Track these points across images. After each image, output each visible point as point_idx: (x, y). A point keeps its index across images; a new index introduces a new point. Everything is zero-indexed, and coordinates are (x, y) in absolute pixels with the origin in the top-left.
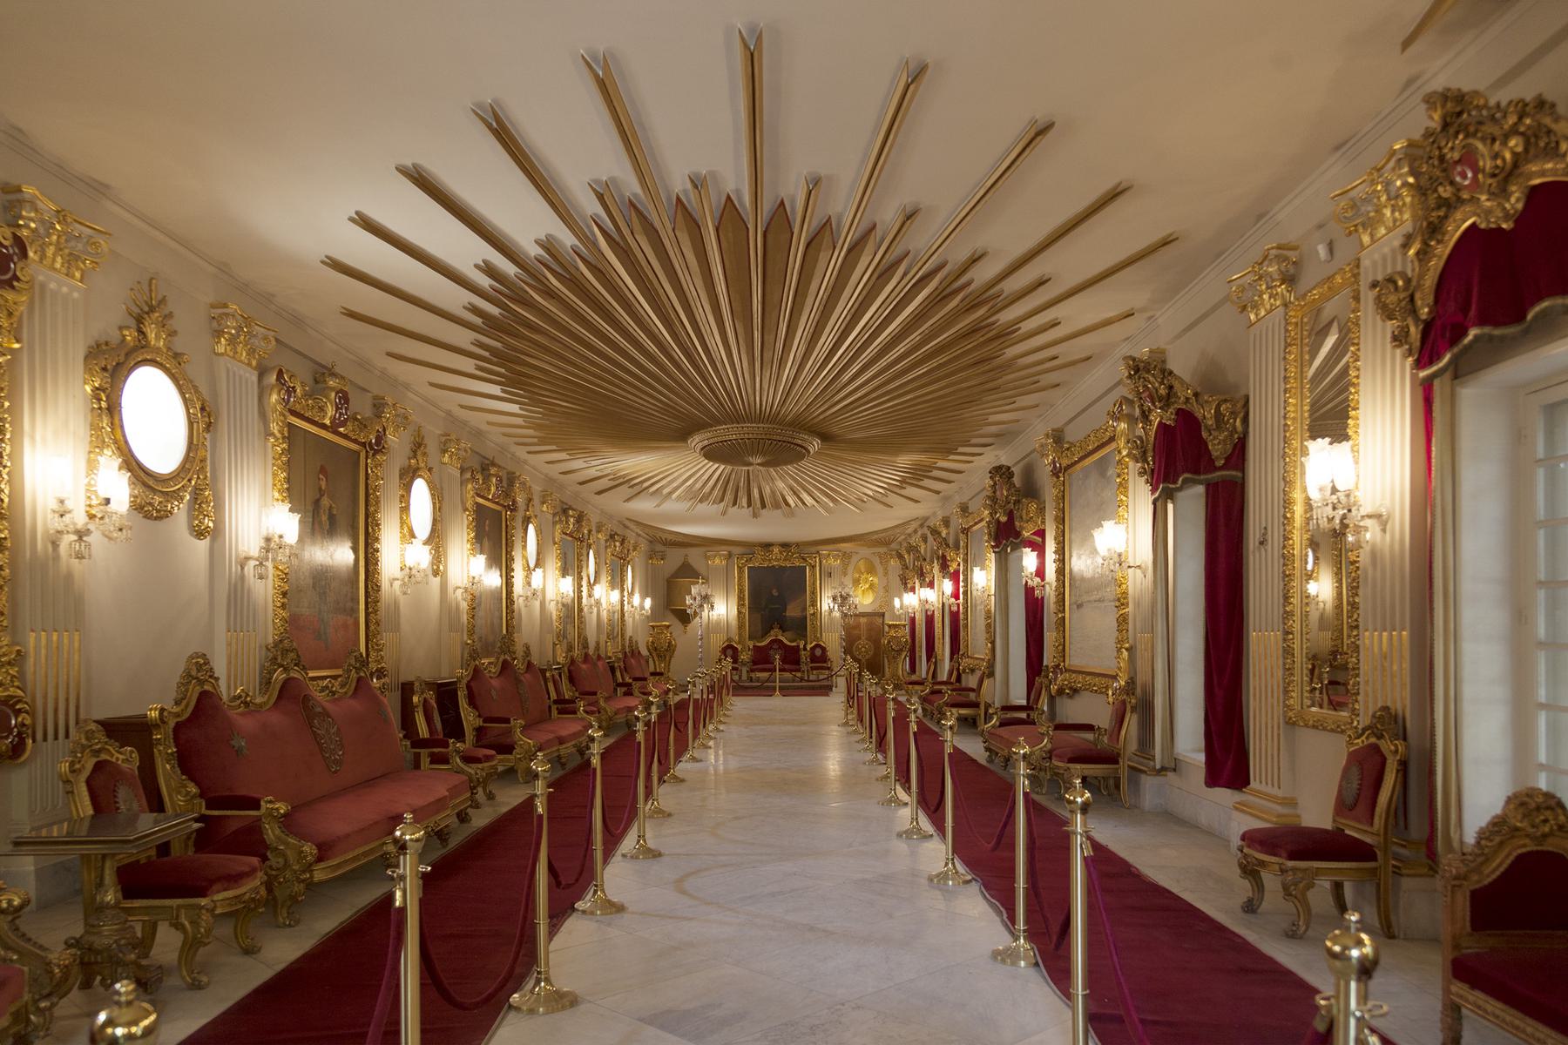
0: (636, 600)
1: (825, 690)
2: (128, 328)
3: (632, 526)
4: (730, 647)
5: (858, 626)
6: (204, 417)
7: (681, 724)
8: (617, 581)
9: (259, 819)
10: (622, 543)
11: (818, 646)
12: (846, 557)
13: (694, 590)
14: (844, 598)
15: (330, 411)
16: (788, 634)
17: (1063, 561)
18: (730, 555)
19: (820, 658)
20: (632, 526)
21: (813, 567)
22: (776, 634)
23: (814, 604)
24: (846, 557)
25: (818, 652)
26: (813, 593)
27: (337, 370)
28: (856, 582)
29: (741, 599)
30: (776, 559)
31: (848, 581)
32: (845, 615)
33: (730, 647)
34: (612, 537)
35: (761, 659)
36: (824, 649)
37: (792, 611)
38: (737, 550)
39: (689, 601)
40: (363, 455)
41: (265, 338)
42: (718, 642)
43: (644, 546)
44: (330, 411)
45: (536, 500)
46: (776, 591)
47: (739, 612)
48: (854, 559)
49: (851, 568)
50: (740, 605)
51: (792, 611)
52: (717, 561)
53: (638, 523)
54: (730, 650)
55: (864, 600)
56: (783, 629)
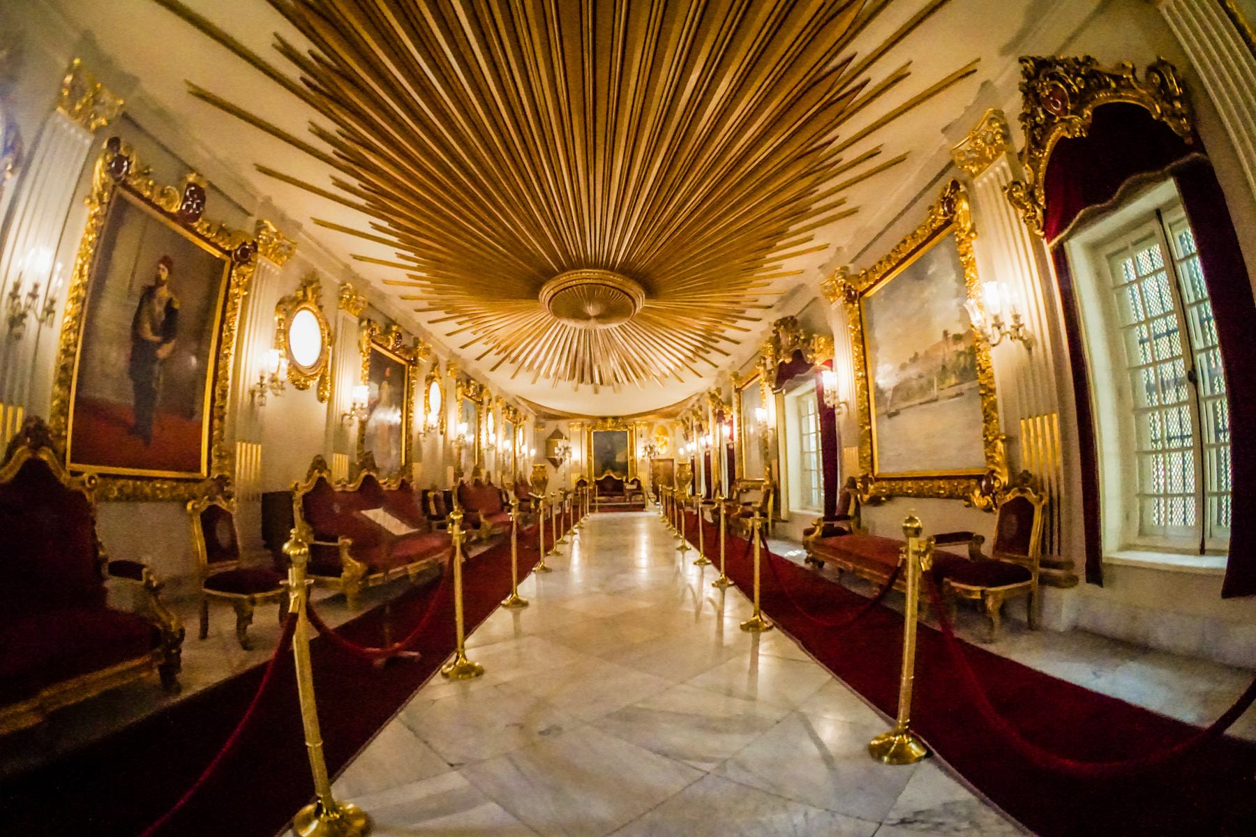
0: (525, 449)
10: (515, 412)
38: (587, 421)
39: (556, 451)
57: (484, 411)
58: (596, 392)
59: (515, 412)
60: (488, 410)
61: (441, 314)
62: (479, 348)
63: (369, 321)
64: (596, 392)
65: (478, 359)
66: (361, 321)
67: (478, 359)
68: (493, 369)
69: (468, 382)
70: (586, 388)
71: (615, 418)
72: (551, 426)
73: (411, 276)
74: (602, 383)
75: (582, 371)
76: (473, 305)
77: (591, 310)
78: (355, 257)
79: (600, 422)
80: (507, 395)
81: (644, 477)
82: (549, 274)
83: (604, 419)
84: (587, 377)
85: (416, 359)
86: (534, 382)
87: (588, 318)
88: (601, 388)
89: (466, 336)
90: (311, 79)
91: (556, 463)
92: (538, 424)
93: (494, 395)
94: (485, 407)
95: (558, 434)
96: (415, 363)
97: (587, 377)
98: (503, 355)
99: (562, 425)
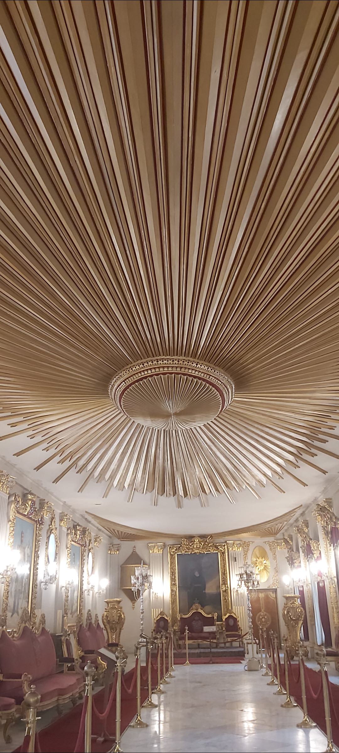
10: (84, 531)
38: (170, 542)
39: (133, 580)
57: (44, 533)
58: (179, 505)
59: (84, 531)
60: (50, 531)
62: (39, 455)
64: (179, 505)
65: (38, 468)
67: (38, 468)
68: (56, 481)
69: (25, 496)
70: (168, 501)
71: (203, 537)
72: (127, 547)
75: (163, 481)
76: (29, 403)
77: (169, 407)
79: (185, 542)
80: (74, 511)
81: (242, 613)
82: (120, 364)
83: (190, 538)
84: (168, 488)
86: (105, 495)
88: (185, 501)
89: (23, 441)
91: (133, 596)
92: (111, 547)
93: (58, 512)
94: (45, 527)
95: (135, 559)
97: (168, 488)
98: (67, 463)
99: (140, 546)
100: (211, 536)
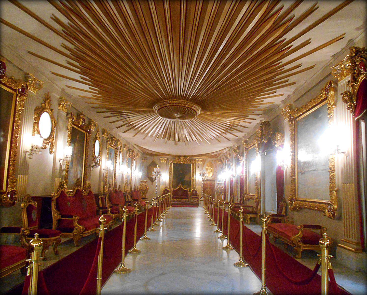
1: (196, 205)
2: (43, 103)
3: (136, 147)
4: (166, 190)
5: (207, 184)
6: (55, 125)
7: (154, 213)
8: (130, 164)
9: (72, 220)
10: (133, 153)
11: (194, 190)
12: (204, 161)
13: (155, 170)
14: (204, 174)
15: (81, 124)
16: (185, 186)
17: (295, 155)
18: (168, 159)
19: (195, 194)
20: (136, 147)
21: (193, 164)
22: (180, 186)
23: (193, 176)
24: (204, 161)
25: (194, 192)
26: (193, 173)
27: (83, 113)
28: (207, 169)
29: (170, 174)
30: (182, 160)
31: (204, 168)
32: (203, 180)
33: (166, 190)
34: (129, 150)
35: (176, 194)
36: (196, 191)
37: (186, 179)
39: (153, 173)
40: (86, 134)
41: (69, 106)
42: (162, 188)
43: (140, 155)
44: (81, 124)
45: (122, 147)
46: (182, 170)
47: (170, 179)
48: (207, 161)
49: (205, 165)
50: (170, 176)
51: (186, 179)
52: (163, 161)
53: (138, 146)
54: (166, 191)
55: (209, 176)
56: (183, 184)
59: (133, 153)
60: (120, 152)
61: (104, 110)
63: (72, 114)
66: (68, 114)
69: (112, 138)
70: (172, 142)
71: (185, 157)
72: (150, 159)
73: (93, 96)
74: (179, 141)
75: (169, 135)
77: (177, 115)
78: (67, 87)
79: (177, 158)
80: (129, 143)
81: (199, 189)
83: (179, 157)
84: (172, 138)
85: (90, 130)
86: (144, 139)
87: (175, 118)
90: (65, 30)
93: (123, 144)
94: (119, 151)
95: (154, 164)
96: (89, 132)
97: (172, 138)
98: (131, 127)
99: (156, 159)
100: (189, 156)
